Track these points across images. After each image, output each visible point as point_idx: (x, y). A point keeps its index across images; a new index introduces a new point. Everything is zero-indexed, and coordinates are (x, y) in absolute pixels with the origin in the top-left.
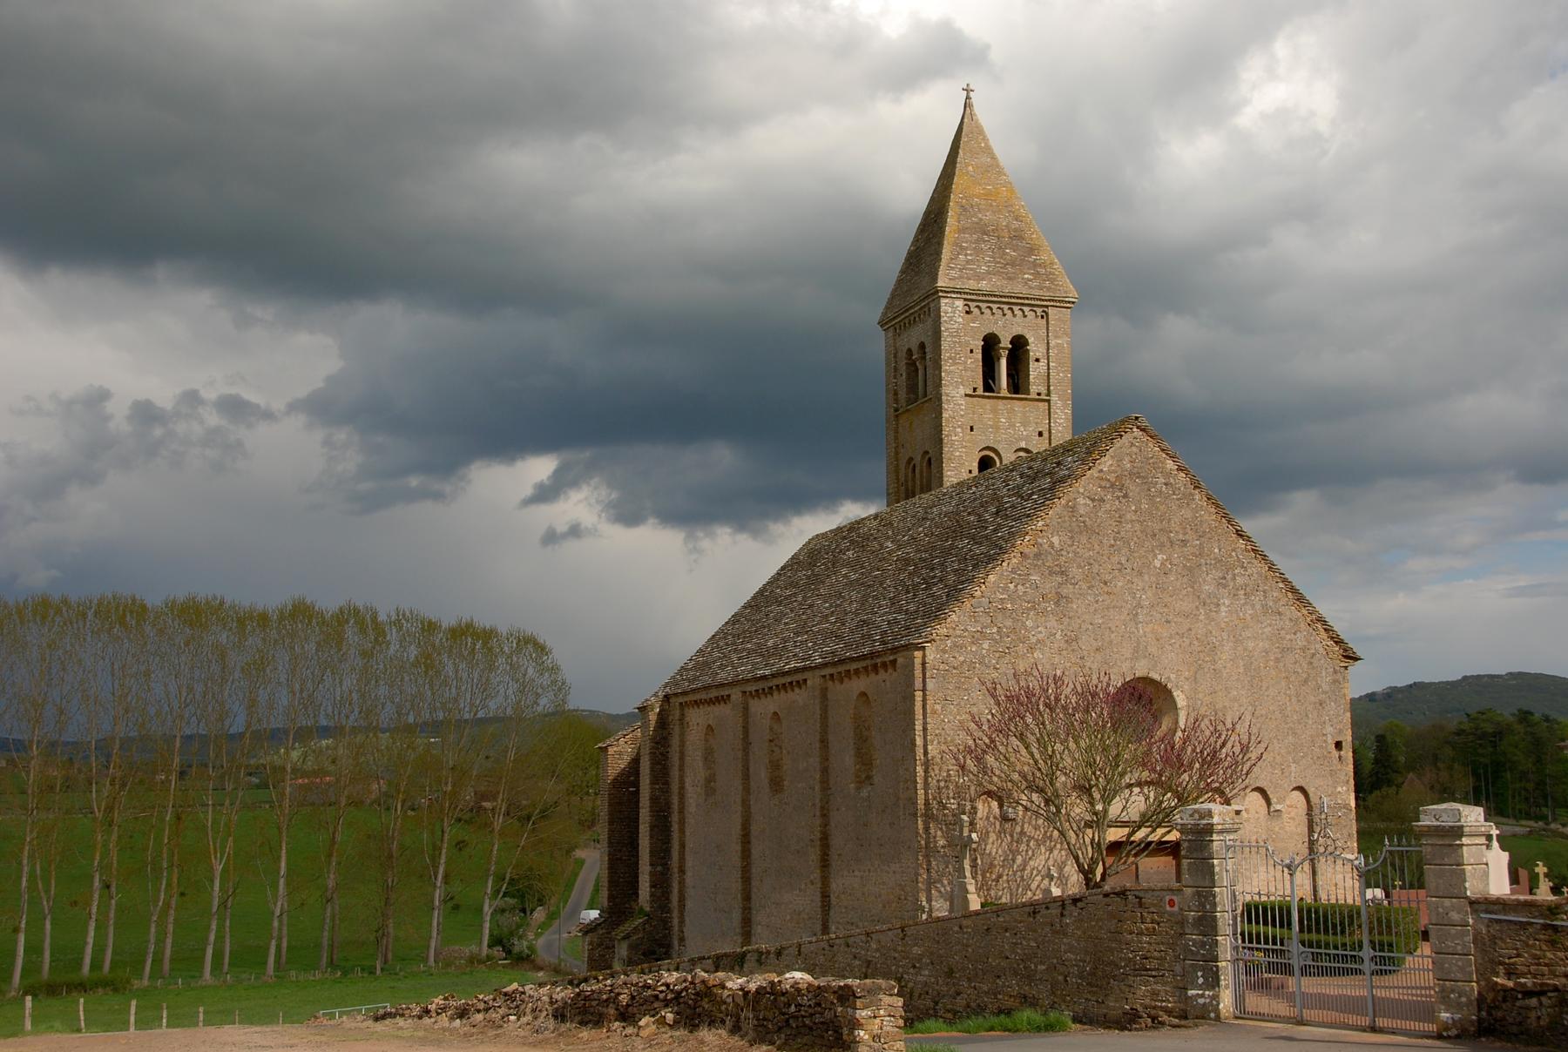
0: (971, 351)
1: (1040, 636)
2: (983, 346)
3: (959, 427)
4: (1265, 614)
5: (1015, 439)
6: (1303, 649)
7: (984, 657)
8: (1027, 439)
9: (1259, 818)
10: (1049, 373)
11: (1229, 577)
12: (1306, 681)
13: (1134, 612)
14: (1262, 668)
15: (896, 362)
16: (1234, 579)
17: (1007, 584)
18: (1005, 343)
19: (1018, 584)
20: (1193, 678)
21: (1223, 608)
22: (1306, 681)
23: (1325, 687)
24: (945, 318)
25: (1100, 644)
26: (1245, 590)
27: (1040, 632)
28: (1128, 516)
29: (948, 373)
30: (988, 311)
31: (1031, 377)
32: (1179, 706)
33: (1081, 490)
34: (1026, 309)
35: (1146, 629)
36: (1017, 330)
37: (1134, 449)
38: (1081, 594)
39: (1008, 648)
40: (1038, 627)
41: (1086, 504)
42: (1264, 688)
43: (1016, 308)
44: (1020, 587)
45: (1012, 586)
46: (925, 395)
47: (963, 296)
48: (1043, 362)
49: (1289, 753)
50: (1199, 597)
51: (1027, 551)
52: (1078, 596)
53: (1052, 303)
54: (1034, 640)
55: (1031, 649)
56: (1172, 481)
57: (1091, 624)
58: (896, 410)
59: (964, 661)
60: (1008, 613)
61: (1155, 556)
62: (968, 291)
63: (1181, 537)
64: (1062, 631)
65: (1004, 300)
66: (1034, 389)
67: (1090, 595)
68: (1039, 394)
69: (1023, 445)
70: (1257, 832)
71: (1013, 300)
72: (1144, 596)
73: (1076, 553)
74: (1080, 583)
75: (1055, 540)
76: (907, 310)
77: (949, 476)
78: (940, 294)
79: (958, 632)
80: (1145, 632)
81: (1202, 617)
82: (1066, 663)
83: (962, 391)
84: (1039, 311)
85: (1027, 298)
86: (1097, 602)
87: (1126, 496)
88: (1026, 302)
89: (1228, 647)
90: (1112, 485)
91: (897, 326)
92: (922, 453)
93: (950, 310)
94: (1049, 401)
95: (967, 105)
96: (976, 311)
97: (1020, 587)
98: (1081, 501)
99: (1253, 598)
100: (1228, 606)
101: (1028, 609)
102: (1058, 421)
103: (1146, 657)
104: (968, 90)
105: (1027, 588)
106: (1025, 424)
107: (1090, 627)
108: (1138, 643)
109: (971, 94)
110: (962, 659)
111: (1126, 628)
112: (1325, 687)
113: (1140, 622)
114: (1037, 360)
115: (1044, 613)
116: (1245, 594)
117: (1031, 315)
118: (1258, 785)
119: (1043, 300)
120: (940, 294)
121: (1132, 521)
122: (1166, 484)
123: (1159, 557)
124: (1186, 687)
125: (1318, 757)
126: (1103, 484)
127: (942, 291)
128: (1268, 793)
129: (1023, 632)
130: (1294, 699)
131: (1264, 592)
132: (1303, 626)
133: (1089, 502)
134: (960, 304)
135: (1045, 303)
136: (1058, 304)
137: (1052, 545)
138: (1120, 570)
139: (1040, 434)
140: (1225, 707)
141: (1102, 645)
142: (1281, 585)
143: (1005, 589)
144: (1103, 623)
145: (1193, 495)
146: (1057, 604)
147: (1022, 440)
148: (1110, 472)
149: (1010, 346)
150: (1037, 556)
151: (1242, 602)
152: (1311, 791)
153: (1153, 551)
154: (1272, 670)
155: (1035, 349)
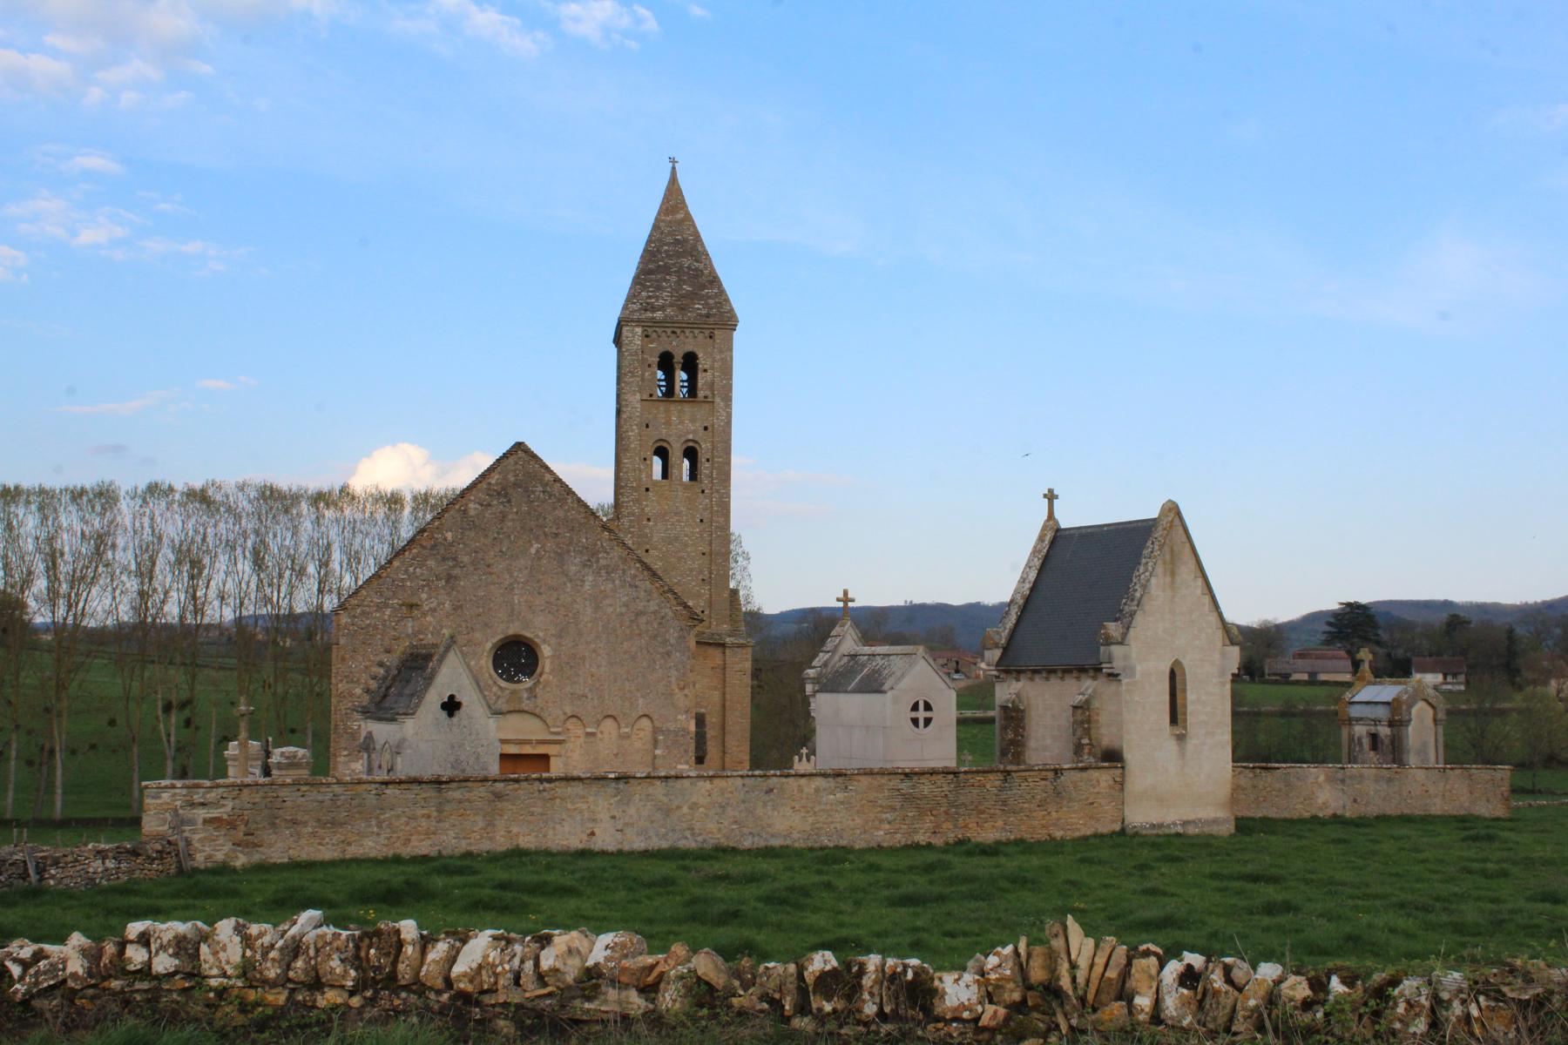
0: (649, 366)
1: (432, 606)
4: (623, 587)
6: (655, 613)
7: (385, 621)
8: (694, 432)
11: (593, 560)
12: (655, 637)
16: (598, 561)
18: (678, 358)
21: (587, 583)
22: (655, 637)
23: (673, 641)
28: (510, 517)
30: (664, 334)
33: (472, 498)
34: (696, 331)
36: (690, 348)
37: (518, 466)
41: (475, 509)
43: (687, 331)
44: (418, 570)
45: (411, 569)
49: (638, 690)
50: (567, 575)
51: (424, 544)
55: (424, 615)
56: (549, 489)
59: (369, 625)
61: (532, 545)
63: (554, 530)
66: (701, 394)
68: (706, 397)
69: (691, 437)
73: (464, 544)
75: (449, 535)
79: (366, 603)
81: (568, 590)
83: (638, 397)
87: (509, 501)
89: (589, 611)
90: (499, 494)
96: (654, 335)
97: (418, 570)
98: (472, 505)
101: (423, 586)
104: (673, 161)
106: (693, 420)
108: (513, 610)
110: (368, 622)
112: (673, 641)
114: (705, 371)
117: (701, 337)
118: (609, 713)
121: (513, 520)
122: (544, 492)
123: (536, 546)
125: (663, 694)
126: (491, 493)
130: (645, 651)
131: (623, 570)
132: (655, 596)
133: (477, 506)
134: (639, 330)
137: (445, 539)
138: (501, 557)
142: (638, 565)
143: (406, 571)
145: (566, 499)
146: (447, 581)
148: (497, 484)
150: (433, 547)
152: (655, 718)
153: (530, 541)
155: (703, 362)
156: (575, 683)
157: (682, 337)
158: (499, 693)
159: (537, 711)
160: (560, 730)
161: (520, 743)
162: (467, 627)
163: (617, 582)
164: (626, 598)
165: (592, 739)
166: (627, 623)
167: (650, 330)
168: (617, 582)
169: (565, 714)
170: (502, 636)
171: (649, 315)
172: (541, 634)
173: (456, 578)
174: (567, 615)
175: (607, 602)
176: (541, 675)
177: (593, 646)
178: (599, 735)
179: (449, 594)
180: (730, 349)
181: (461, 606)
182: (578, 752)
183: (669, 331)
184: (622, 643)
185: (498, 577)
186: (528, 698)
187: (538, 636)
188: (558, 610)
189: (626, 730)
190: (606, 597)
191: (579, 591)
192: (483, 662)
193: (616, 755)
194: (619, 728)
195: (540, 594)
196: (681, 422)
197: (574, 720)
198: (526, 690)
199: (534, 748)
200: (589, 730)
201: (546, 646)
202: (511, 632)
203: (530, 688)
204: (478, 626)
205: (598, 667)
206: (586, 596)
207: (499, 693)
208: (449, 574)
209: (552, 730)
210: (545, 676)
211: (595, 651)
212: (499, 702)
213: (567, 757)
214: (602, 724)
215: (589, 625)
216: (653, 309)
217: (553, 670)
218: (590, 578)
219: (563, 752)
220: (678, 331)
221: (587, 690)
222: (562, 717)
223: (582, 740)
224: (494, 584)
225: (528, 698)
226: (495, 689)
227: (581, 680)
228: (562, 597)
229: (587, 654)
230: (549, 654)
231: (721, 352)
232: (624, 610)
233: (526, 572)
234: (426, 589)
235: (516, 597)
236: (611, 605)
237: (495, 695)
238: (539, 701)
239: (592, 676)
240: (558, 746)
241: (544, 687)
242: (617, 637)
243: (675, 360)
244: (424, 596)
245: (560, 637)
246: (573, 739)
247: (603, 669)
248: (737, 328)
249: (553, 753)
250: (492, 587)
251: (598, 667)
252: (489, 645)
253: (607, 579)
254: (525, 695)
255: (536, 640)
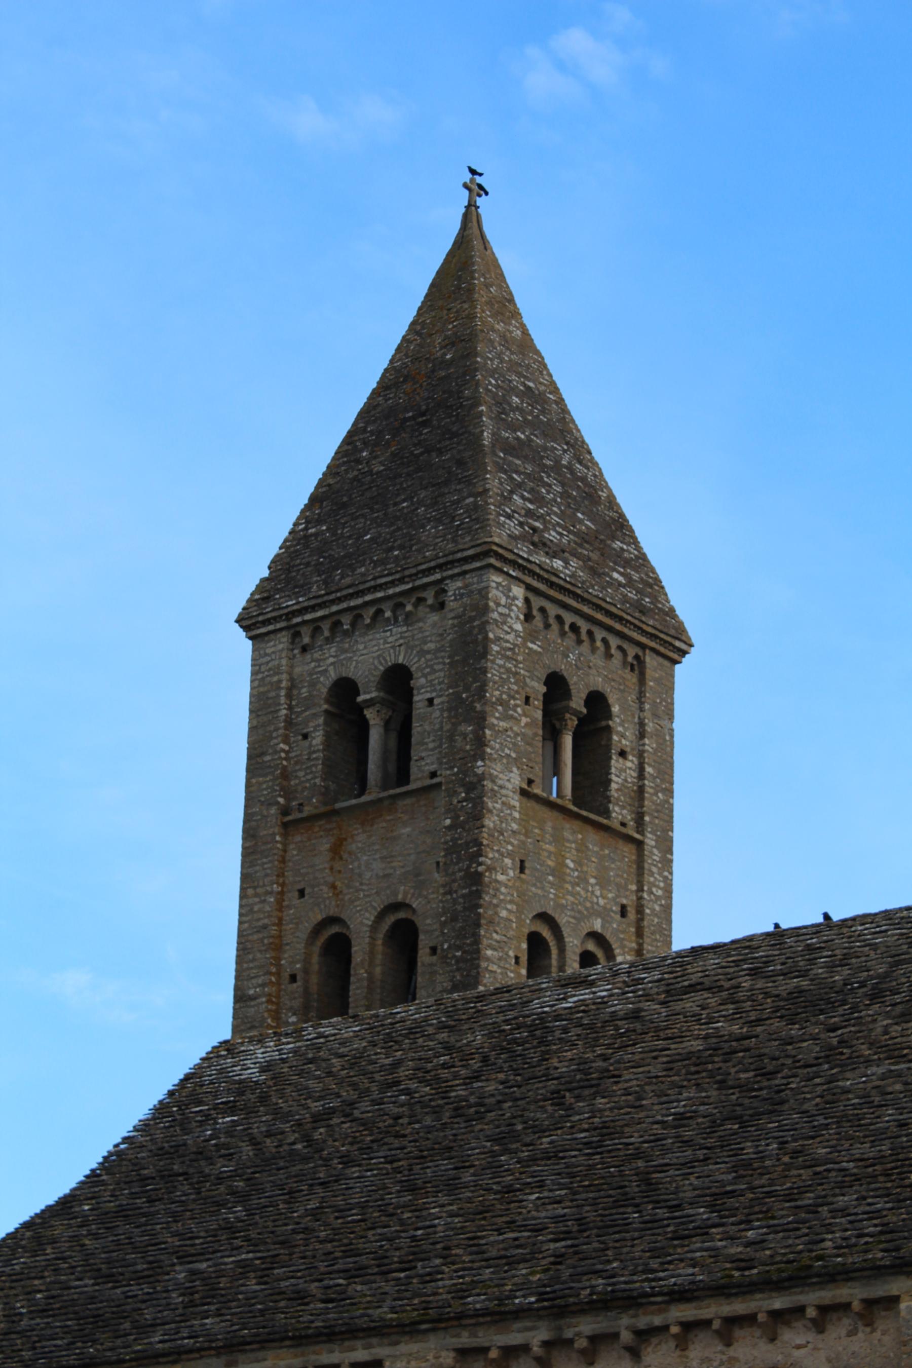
2: (545, 695)
3: (510, 855)
5: (587, 909)
8: (604, 913)
10: (641, 790)
15: (290, 708)
24: (495, 615)
29: (497, 733)
31: (614, 786)
34: (614, 642)
36: (598, 682)
46: (403, 776)
47: (529, 580)
48: (631, 763)
53: (652, 644)
58: (285, 811)
62: (538, 570)
65: (586, 609)
71: (599, 616)
76: (361, 593)
77: (488, 959)
78: (492, 561)
84: (632, 651)
85: (620, 619)
88: (618, 626)
91: (346, 621)
92: (378, 904)
93: (503, 601)
94: (640, 844)
95: (471, 216)
96: (538, 621)
102: (654, 890)
104: (476, 190)
106: (603, 883)
109: (480, 201)
114: (623, 754)
119: (644, 633)
120: (492, 561)
127: (496, 553)
135: (644, 640)
136: (662, 650)
139: (623, 912)
147: (598, 914)
149: (585, 711)
157: (585, 647)
167: (537, 602)
171: (540, 558)
180: (671, 718)
183: (569, 618)
196: (582, 880)
216: (541, 545)
220: (584, 626)
231: (656, 715)
243: (573, 705)
248: (686, 659)
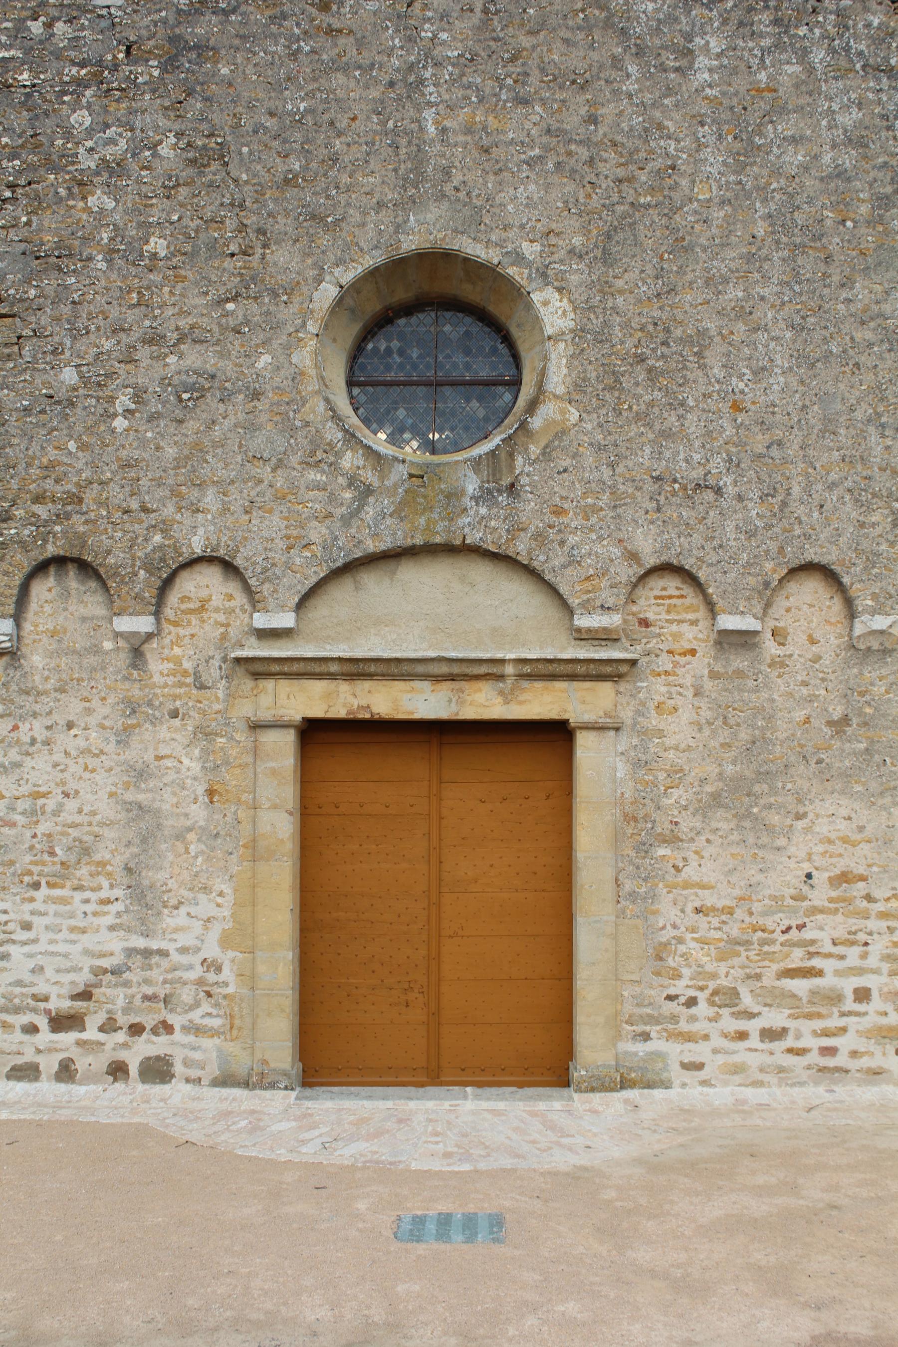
1: (109, 153)
4: (841, 73)
9: (817, 659)
13: (412, 79)
14: (829, 223)
17: (24, 20)
19: (55, 20)
20: (599, 253)
21: (702, 61)
25: (297, 167)
26: (777, 8)
27: (112, 142)
32: (549, 331)
35: (447, 123)
38: (243, 38)
39: (12, 186)
40: (107, 126)
42: (836, 278)
44: (60, 27)
45: (36, 28)
52: (237, 42)
54: (90, 163)
57: (271, 114)
60: (18, 96)
64: (179, 135)
67: (275, 37)
70: (811, 699)
72: (444, 36)
74: (243, 8)
80: (444, 130)
81: (630, 86)
82: (186, 221)
86: (295, 55)
97: (60, 27)
99: (802, 31)
100: (719, 56)
101: (80, 83)
103: (444, 196)
105: (83, 28)
107: (270, 123)
108: (419, 159)
111: (384, 123)
113: (430, 104)
115: (127, 91)
116: (776, 22)
118: (812, 554)
124: (574, 279)
128: (846, 580)
129: (59, 142)
140: (702, 333)
141: (305, 168)
144: (308, 111)
146: (169, 64)
151: (766, 42)
154: (864, 231)
156: (666, 434)
158: (370, 477)
159: (521, 548)
160: (613, 620)
161: (452, 678)
162: (242, 227)
163: (818, 56)
164: (856, 114)
165: (739, 662)
166: (864, 209)
168: (818, 56)
169: (633, 556)
170: (369, 262)
172: (530, 250)
173: (202, 49)
174: (630, 180)
175: (786, 127)
176: (532, 406)
177: (736, 293)
178: (771, 648)
179: (176, 108)
181: (221, 154)
182: (686, 715)
184: (846, 283)
185: (360, 45)
186: (485, 496)
187: (519, 259)
188: (591, 162)
189: (880, 622)
190: (777, 110)
191: (670, 91)
192: (303, 357)
193: (840, 725)
194: (851, 611)
195: (524, 102)
197: (671, 584)
198: (476, 464)
199: (507, 698)
200: (729, 622)
201: (550, 293)
202: (410, 244)
203: (492, 453)
204: (284, 224)
205: (759, 372)
206: (704, 108)
207: (370, 477)
208: (173, 40)
209: (583, 621)
210: (548, 411)
211: (742, 313)
212: (369, 512)
213: (644, 734)
214: (781, 604)
215: (718, 214)
217: (579, 386)
218: (715, 44)
219: (626, 715)
221: (717, 464)
222: (626, 572)
223: (700, 665)
224: (345, 69)
225: (485, 496)
226: (350, 460)
227: (693, 424)
228: (607, 111)
229: (711, 326)
230: (567, 323)
232: (848, 159)
233: (465, 25)
234: (88, 93)
235: (429, 115)
236: (795, 140)
237: (352, 482)
238: (528, 507)
239: (737, 407)
240: (606, 688)
241: (547, 453)
242: (828, 259)
244: (81, 119)
245: (607, 259)
246: (665, 662)
247: (778, 381)
249: (588, 717)
250: (340, 79)
251: (759, 372)
252: (328, 292)
253: (778, 46)
254: (472, 486)
255: (512, 271)
